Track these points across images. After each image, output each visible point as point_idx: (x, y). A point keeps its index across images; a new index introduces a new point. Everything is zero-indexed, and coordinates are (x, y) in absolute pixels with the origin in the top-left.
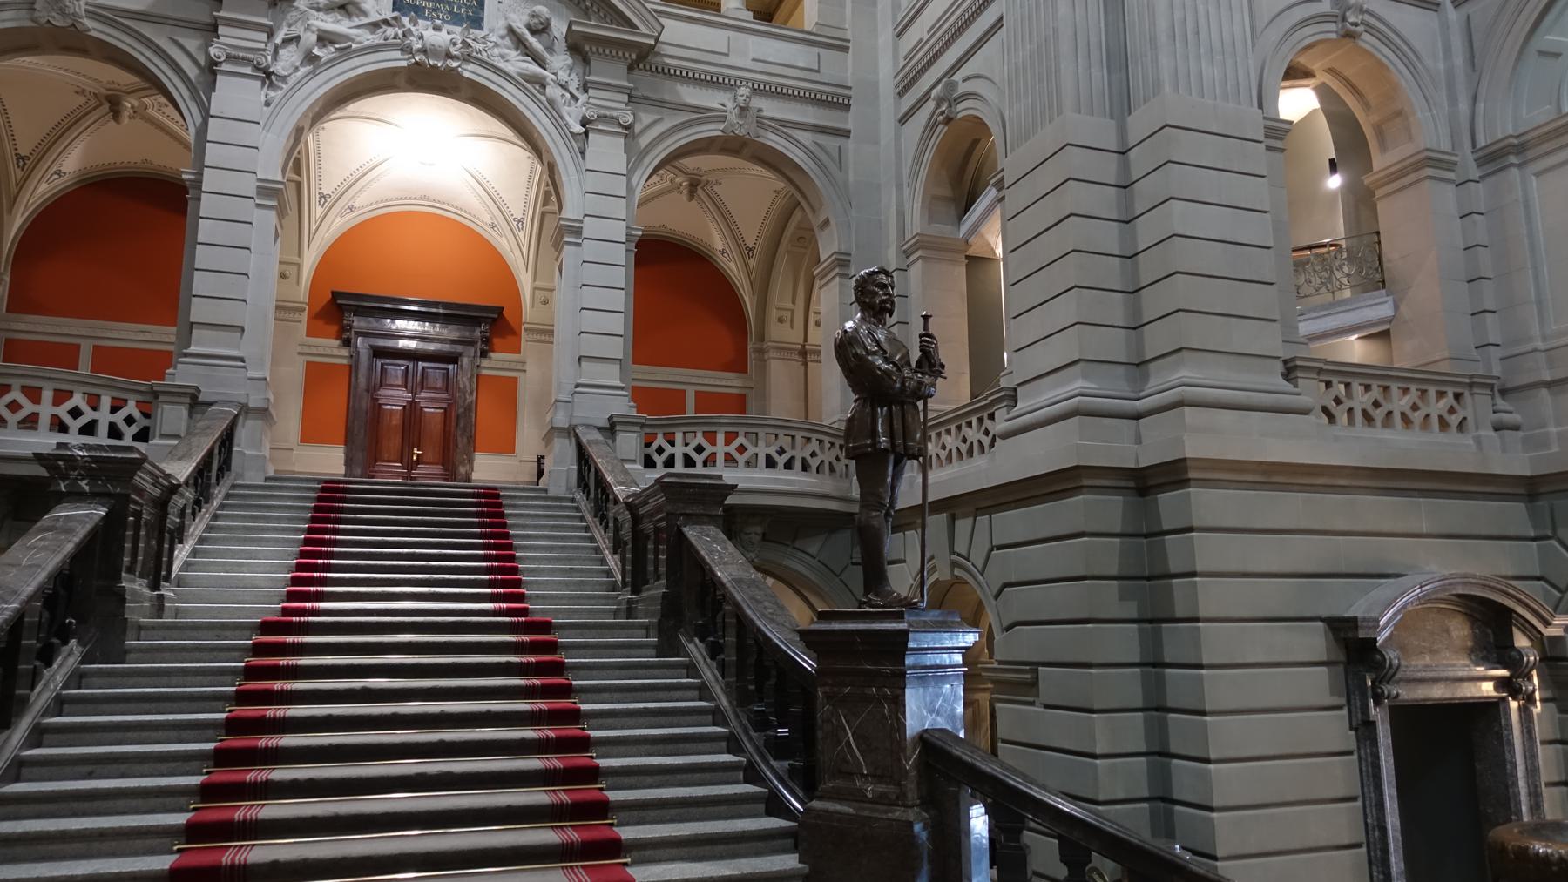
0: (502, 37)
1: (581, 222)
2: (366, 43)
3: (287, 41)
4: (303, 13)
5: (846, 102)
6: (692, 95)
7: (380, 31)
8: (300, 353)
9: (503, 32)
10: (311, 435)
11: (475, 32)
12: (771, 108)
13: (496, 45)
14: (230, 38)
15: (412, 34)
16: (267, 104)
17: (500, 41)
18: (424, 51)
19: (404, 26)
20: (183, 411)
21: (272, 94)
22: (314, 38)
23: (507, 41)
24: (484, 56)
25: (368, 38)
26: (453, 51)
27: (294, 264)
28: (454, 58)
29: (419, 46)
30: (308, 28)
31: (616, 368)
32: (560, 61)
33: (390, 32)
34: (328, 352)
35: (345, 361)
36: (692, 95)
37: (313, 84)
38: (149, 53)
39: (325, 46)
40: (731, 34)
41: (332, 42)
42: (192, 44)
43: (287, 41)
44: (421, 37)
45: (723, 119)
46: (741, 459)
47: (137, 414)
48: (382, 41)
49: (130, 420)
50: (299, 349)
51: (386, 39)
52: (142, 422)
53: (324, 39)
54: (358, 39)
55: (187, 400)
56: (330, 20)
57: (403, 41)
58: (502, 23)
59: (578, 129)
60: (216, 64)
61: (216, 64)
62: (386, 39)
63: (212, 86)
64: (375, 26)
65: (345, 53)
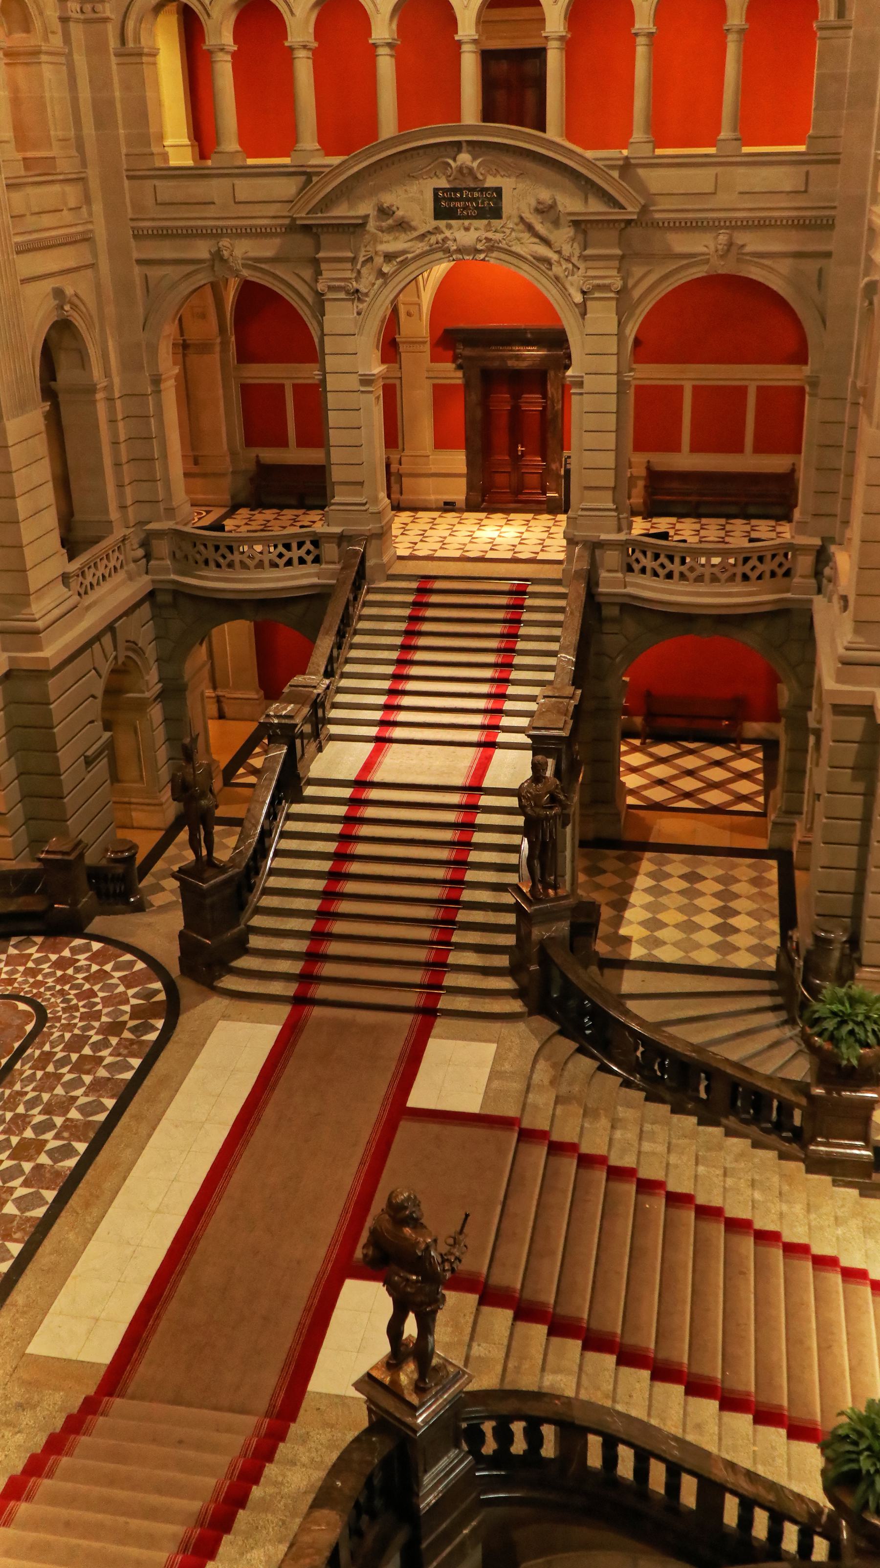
0: (517, 224)
1: (582, 377)
2: (418, 252)
3: (364, 263)
4: (373, 235)
5: (830, 222)
6: (682, 243)
7: (427, 239)
8: (427, 378)
9: (517, 220)
10: (441, 443)
11: (496, 223)
12: (752, 242)
13: (513, 230)
14: (329, 273)
15: (449, 239)
16: (359, 313)
17: (516, 228)
18: (459, 251)
19: (443, 232)
20: (335, 546)
21: (361, 306)
22: (382, 259)
23: (521, 227)
24: (503, 245)
25: (421, 247)
26: (479, 247)
27: (415, 304)
28: (480, 251)
29: (455, 248)
30: (376, 253)
31: (609, 494)
32: (563, 236)
33: (433, 239)
34: (449, 375)
35: (459, 382)
36: (682, 243)
37: (385, 292)
38: (282, 287)
39: (390, 261)
40: (719, 169)
41: (397, 257)
42: (307, 274)
43: (364, 263)
44: (455, 240)
45: (707, 261)
46: (692, 576)
47: (312, 548)
48: (428, 248)
49: (308, 552)
50: (426, 375)
51: (431, 246)
52: (315, 552)
53: (389, 257)
54: (412, 250)
55: (336, 540)
56: (391, 238)
57: (443, 245)
58: (515, 213)
59: (578, 298)
60: (323, 295)
61: (323, 295)
62: (431, 246)
63: (323, 314)
64: (422, 237)
65: (404, 263)
